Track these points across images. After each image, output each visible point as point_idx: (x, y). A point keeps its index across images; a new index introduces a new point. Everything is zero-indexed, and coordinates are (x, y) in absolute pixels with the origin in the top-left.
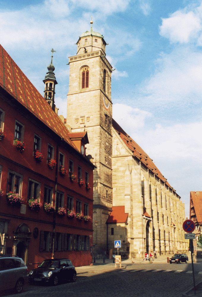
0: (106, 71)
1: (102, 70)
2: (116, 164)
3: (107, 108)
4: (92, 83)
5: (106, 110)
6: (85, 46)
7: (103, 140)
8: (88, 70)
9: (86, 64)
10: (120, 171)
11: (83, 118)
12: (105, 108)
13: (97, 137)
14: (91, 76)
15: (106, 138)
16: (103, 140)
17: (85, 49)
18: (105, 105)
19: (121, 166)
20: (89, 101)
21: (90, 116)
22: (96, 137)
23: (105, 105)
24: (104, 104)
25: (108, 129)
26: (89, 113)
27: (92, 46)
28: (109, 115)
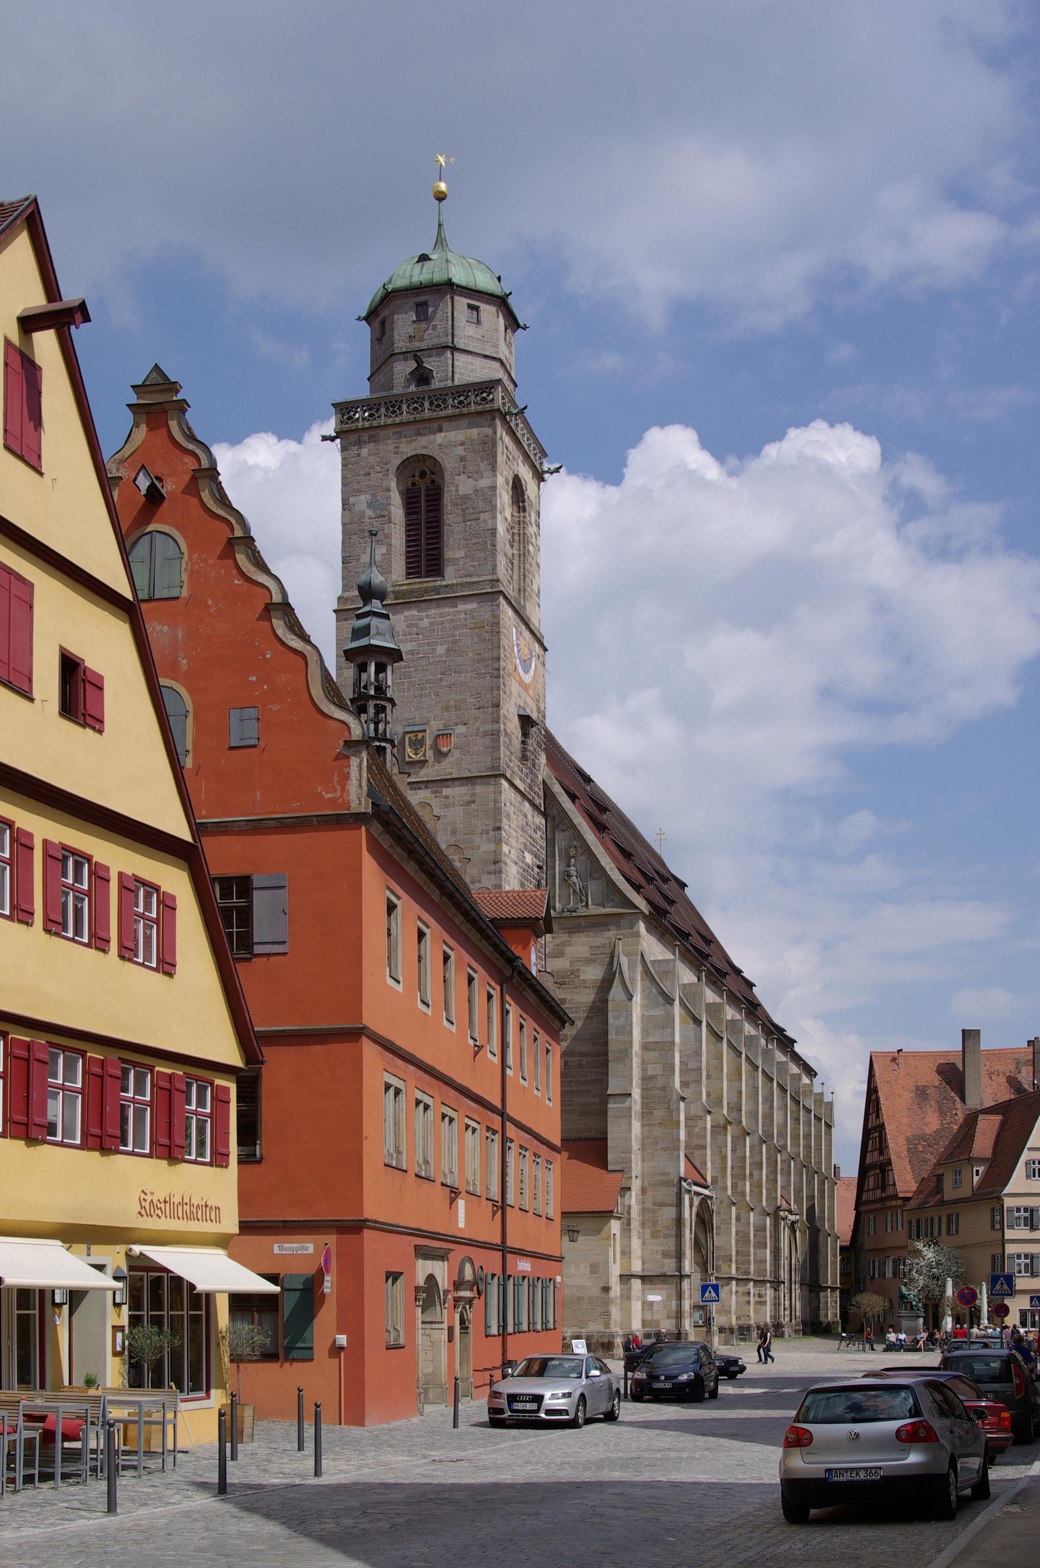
0: (520, 481)
1: (507, 483)
2: (568, 950)
3: (527, 679)
4: (461, 554)
5: (523, 693)
6: (417, 345)
7: (514, 844)
8: (433, 482)
9: (425, 447)
10: (585, 981)
11: (420, 736)
12: (521, 683)
13: (492, 833)
14: (450, 516)
15: (523, 830)
16: (514, 844)
17: (420, 363)
18: (520, 668)
19: (588, 961)
20: (448, 650)
21: (457, 724)
22: (487, 833)
23: (520, 668)
24: (518, 661)
25: (530, 787)
26: (447, 709)
27: (454, 349)
28: (535, 711)
